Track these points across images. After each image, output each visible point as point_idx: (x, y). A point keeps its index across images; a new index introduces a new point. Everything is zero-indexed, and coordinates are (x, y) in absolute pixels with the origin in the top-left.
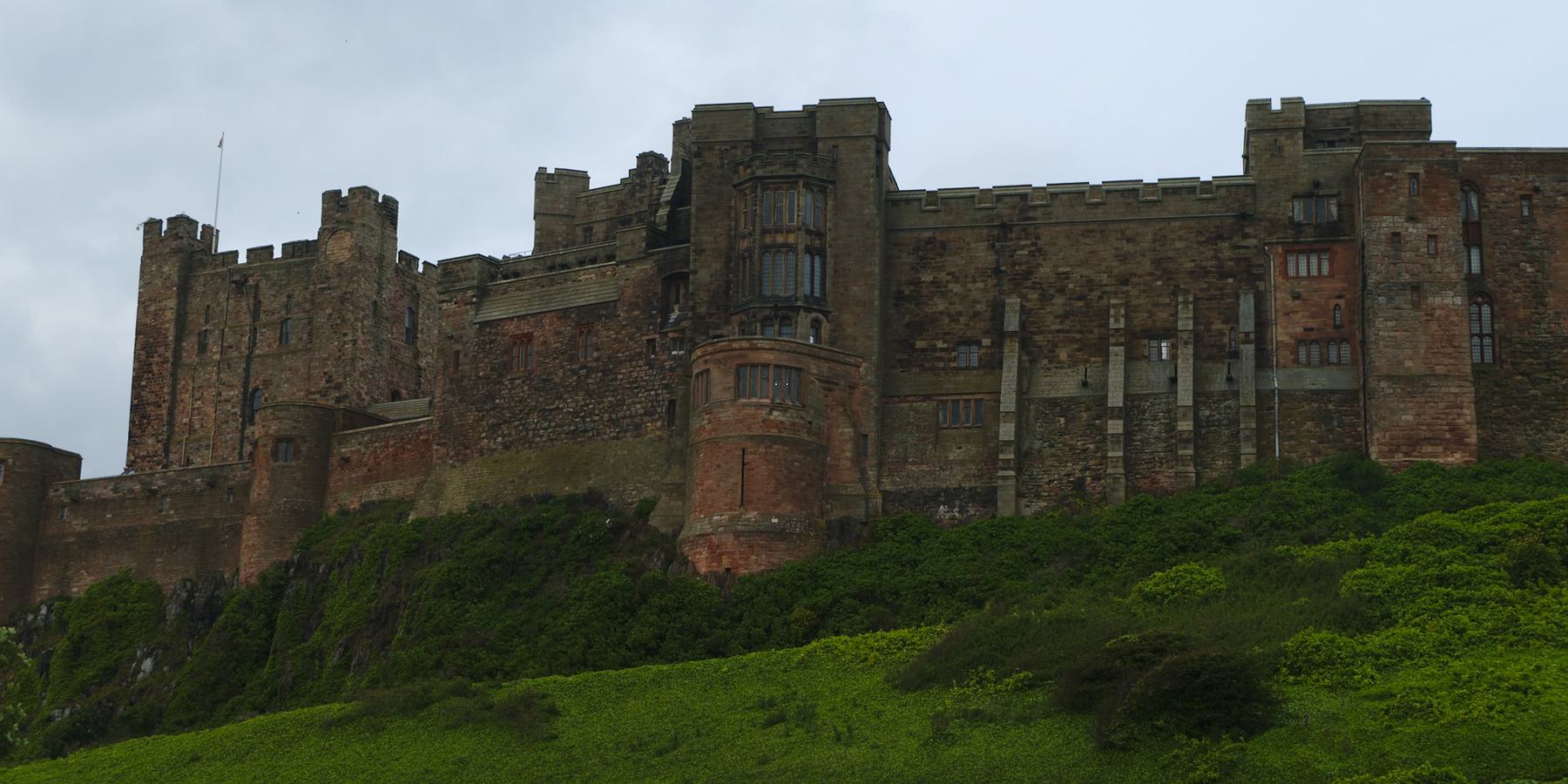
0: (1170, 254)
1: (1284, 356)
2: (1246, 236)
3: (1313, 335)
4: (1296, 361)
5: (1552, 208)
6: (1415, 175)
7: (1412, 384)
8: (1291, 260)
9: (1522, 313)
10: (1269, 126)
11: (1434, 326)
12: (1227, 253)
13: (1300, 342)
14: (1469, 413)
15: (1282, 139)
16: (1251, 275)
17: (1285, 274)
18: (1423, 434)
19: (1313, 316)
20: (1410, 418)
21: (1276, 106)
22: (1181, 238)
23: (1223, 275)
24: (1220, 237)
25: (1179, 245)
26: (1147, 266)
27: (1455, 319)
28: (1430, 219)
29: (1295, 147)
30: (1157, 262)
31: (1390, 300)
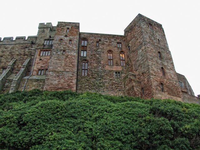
0: (14, 51)
1: (35, 73)
2: (32, 47)
3: (42, 68)
4: (37, 74)
5: (103, 44)
6: (68, 28)
7: (59, 74)
8: (42, 52)
9: (95, 65)
10: (43, 27)
11: (68, 59)
12: (27, 51)
13: (39, 70)
14: (74, 81)
15: (45, 30)
16: (31, 55)
17: (39, 55)
18: (60, 87)
19: (43, 64)
20: (56, 82)
21: (45, 24)
22: (17, 48)
23: (25, 55)
24: (26, 48)
25: (17, 49)
26: (8, 53)
27: (74, 58)
28: (70, 37)
29: (47, 31)
30: (10, 53)
31: (57, 53)
